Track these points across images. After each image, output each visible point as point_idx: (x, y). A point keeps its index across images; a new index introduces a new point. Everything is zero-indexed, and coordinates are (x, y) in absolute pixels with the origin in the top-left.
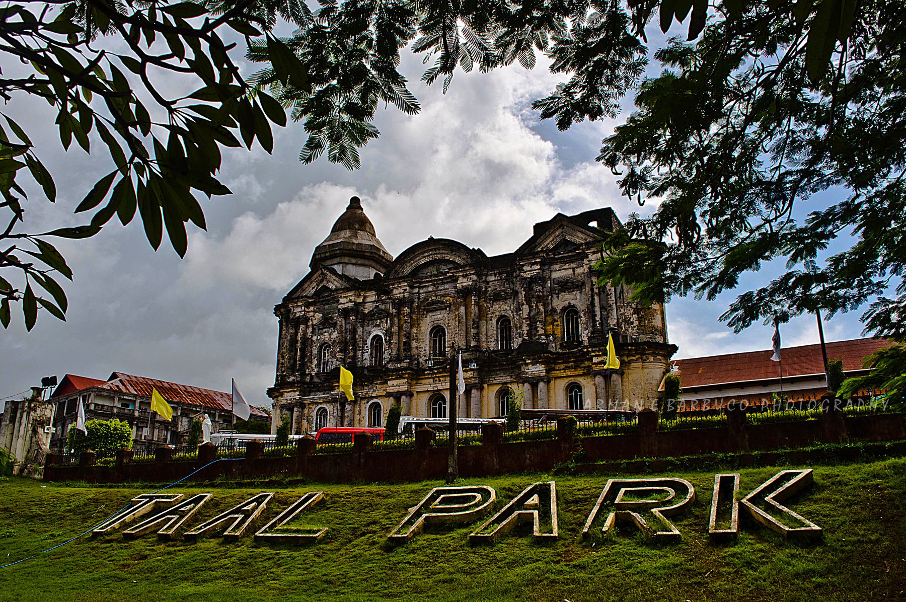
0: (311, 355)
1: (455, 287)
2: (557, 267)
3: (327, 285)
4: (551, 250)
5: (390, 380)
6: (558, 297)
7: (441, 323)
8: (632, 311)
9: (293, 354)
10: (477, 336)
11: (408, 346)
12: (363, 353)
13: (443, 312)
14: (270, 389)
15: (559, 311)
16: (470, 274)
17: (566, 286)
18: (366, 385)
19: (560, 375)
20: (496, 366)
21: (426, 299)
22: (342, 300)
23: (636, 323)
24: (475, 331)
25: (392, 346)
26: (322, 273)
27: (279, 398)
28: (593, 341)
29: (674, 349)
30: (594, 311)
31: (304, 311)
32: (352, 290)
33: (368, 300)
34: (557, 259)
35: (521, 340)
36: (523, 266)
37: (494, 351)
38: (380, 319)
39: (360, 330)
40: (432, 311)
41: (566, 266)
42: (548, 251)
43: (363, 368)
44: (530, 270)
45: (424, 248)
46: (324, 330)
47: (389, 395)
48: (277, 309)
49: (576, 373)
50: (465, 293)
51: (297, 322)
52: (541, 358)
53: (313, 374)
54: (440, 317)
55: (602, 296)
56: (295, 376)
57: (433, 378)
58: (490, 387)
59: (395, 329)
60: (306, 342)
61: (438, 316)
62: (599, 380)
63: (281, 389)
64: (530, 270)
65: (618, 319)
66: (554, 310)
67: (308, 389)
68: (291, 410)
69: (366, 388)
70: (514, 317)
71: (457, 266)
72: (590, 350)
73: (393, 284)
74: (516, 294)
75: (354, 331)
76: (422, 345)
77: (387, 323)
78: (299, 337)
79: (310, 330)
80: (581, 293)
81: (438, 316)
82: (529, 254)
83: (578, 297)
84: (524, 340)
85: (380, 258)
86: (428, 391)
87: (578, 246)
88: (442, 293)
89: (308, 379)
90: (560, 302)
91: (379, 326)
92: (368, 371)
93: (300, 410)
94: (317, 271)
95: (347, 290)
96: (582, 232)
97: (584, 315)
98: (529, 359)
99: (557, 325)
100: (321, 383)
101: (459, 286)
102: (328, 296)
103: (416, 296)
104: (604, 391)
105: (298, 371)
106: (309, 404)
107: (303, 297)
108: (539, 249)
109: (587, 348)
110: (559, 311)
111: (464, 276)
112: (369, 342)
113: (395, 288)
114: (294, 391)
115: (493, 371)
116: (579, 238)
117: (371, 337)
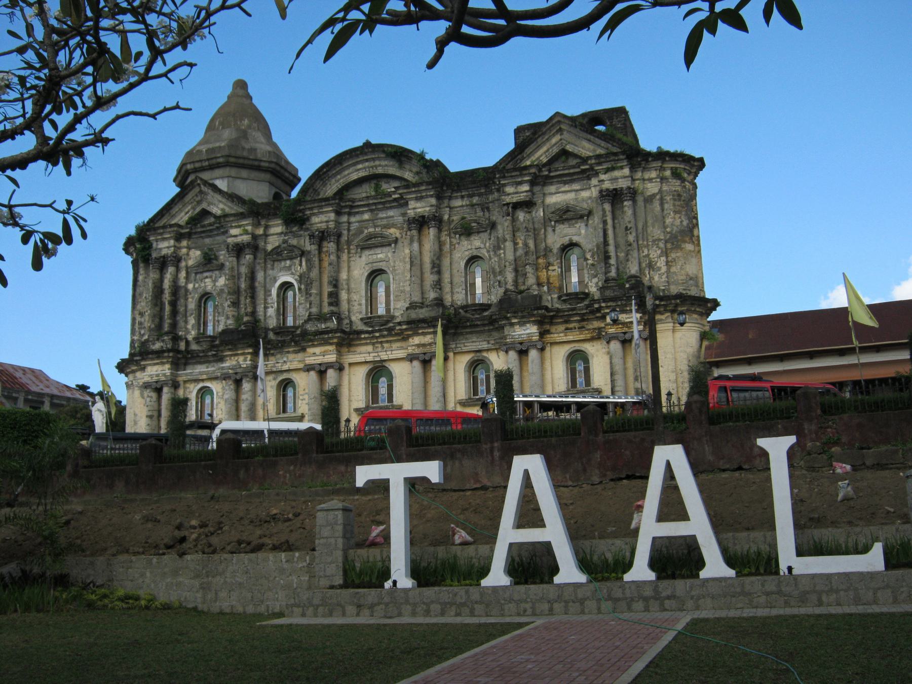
0: (186, 311)
1: (404, 215)
2: (552, 189)
3: (208, 209)
4: (544, 165)
5: (309, 346)
6: (554, 230)
7: (382, 265)
8: (659, 252)
9: (158, 309)
10: (438, 285)
11: (334, 298)
12: (266, 308)
14: (123, 360)
15: (555, 251)
16: (427, 196)
17: (566, 215)
18: (273, 355)
19: (558, 340)
20: (466, 327)
21: (360, 231)
22: (234, 232)
23: (664, 269)
24: (435, 277)
25: (312, 298)
26: (201, 192)
27: (138, 374)
28: (609, 293)
29: (715, 304)
30: (606, 252)
31: (175, 246)
32: (249, 217)
33: (273, 230)
34: (553, 177)
35: (501, 291)
36: (505, 185)
37: (463, 307)
38: (291, 259)
39: (260, 276)
40: (369, 248)
41: (566, 188)
42: (540, 167)
43: (267, 330)
44: (517, 191)
45: (357, 156)
46: (206, 274)
47: (308, 368)
48: (129, 245)
49: (582, 337)
50: (420, 223)
51: (163, 263)
52: (534, 315)
53: (190, 338)
54: (381, 255)
55: (617, 230)
56: (163, 341)
57: (373, 344)
58: (458, 357)
59: (314, 274)
60: (176, 290)
61: (380, 256)
62: (615, 346)
64: (517, 191)
65: (640, 264)
66: (548, 250)
67: (183, 361)
68: (159, 391)
69: (271, 358)
70: (490, 258)
71: (407, 185)
72: (603, 305)
73: (311, 209)
74: (493, 226)
75: (252, 277)
76: (355, 297)
77: (301, 265)
78: (167, 284)
79: (183, 274)
80: (586, 225)
81: (380, 256)
82: (515, 169)
83: (583, 232)
84: (507, 291)
85: (282, 171)
86: (366, 362)
87: (585, 160)
88: (384, 222)
89: (182, 346)
90: (557, 237)
91: (289, 268)
92: (276, 334)
93: (172, 390)
94: (193, 188)
95: (241, 216)
96: (589, 140)
97: (592, 256)
98: (515, 317)
99: (553, 270)
100: (203, 351)
101: (411, 213)
102: (210, 225)
103: (345, 226)
104: (621, 362)
105: (167, 333)
106: (185, 382)
107: (171, 226)
108: (528, 163)
109: (599, 303)
110: (555, 251)
111: (418, 199)
112: (274, 292)
113: (314, 214)
114: (163, 363)
115: (462, 334)
116: (585, 148)
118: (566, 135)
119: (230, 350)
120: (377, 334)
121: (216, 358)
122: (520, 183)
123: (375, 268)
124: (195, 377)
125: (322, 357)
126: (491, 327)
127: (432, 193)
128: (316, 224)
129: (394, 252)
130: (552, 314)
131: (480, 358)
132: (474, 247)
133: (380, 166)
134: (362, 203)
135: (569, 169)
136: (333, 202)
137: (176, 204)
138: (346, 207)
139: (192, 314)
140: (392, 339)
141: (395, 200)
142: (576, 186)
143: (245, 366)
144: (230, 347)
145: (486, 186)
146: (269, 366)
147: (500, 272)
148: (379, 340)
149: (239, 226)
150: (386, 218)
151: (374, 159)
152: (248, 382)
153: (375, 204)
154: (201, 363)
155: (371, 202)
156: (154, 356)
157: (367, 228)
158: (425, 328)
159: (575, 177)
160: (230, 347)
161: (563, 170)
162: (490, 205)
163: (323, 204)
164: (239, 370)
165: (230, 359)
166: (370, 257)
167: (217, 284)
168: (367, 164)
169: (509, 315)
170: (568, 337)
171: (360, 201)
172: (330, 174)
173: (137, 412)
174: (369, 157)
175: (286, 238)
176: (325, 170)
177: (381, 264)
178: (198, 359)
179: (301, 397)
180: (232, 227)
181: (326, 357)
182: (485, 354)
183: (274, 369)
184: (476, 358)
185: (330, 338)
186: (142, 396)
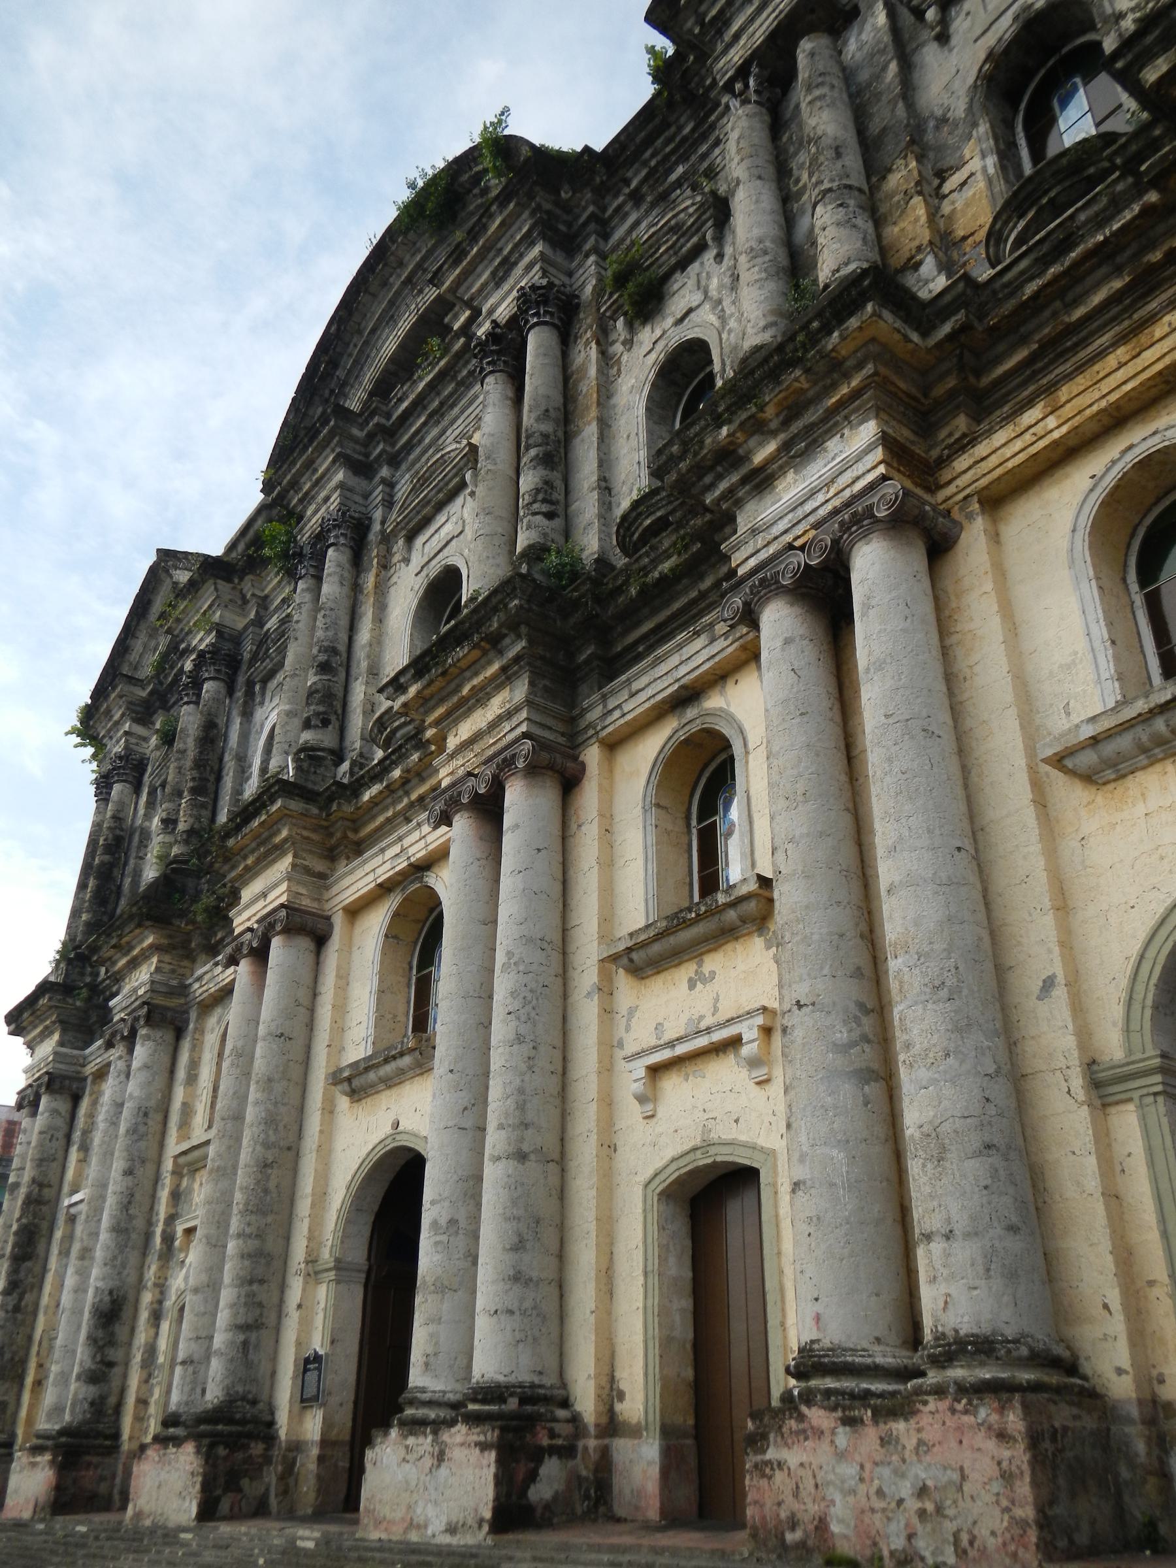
45: (385, 284)
52: (837, 369)
123: (432, 575)
129: (472, 494)
130: (946, 328)
132: (670, 321)
134: (405, 404)
137: (134, 636)
138: (371, 436)
152: (147, 1038)
153: (432, 387)
158: (474, 667)
170: (1068, 411)
172: (340, 373)
174: (410, 268)
180: (190, 632)
181: (271, 897)
182: (714, 702)
184: (682, 735)
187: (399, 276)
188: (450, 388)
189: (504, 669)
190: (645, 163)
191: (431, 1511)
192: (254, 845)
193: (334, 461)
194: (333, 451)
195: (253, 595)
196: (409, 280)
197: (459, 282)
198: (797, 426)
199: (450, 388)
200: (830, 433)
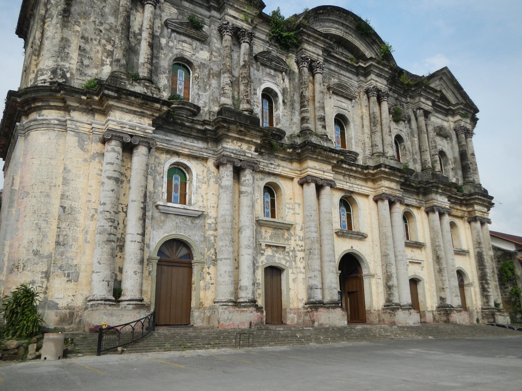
5: (312, 159)
13: (348, 102)
17: (441, 133)
27: (76, 115)
36: (421, 95)
38: (275, 70)
41: (436, 114)
46: (183, 38)
56: (147, 87)
57: (344, 176)
61: (343, 104)
63: (113, 98)
70: (407, 141)
73: (309, 36)
83: (446, 146)
96: (454, 93)
98: (442, 188)
112: (259, 93)
113: (308, 42)
114: (142, 115)
117: (263, 87)
118: (442, 82)
119: (240, 132)
120: (354, 168)
121: (199, 135)
122: (428, 99)
123: (341, 113)
124: (174, 148)
125: (322, 173)
126: (415, 191)
127: (387, 76)
128: (310, 51)
131: (409, 211)
133: (351, 35)
135: (443, 104)
136: (329, 41)
139: (165, 73)
140: (359, 176)
141: (360, 66)
142: (440, 116)
143: (250, 156)
144: (242, 129)
145: (405, 91)
146: (262, 164)
147: (416, 152)
148: (351, 174)
149: (242, 12)
150: (348, 77)
151: (347, 27)
153: (343, 62)
154: (177, 133)
155: (343, 59)
156: (139, 101)
157: (333, 77)
158: (396, 176)
159: (442, 111)
160: (242, 129)
161: (441, 103)
162: (404, 104)
163: (322, 38)
164: (242, 158)
165: (232, 142)
166: (337, 101)
167: (197, 55)
168: (341, 28)
169: (441, 186)
171: (336, 53)
173: (69, 167)
174: (346, 23)
175: (271, 49)
176: (321, 11)
177: (344, 111)
178: (178, 128)
179: (288, 206)
180: (232, 7)
181: (326, 174)
183: (267, 170)
185: (334, 158)
186: (81, 146)
187: (343, 20)
188: (345, 67)
189: (398, 181)
190: (395, 88)
191: (410, 321)
192: (324, 156)
193: (322, 47)
194: (324, 45)
195: (256, 25)
196: (343, 24)
197: (374, 66)
198: (444, 192)
199: (345, 67)
200: (444, 195)
